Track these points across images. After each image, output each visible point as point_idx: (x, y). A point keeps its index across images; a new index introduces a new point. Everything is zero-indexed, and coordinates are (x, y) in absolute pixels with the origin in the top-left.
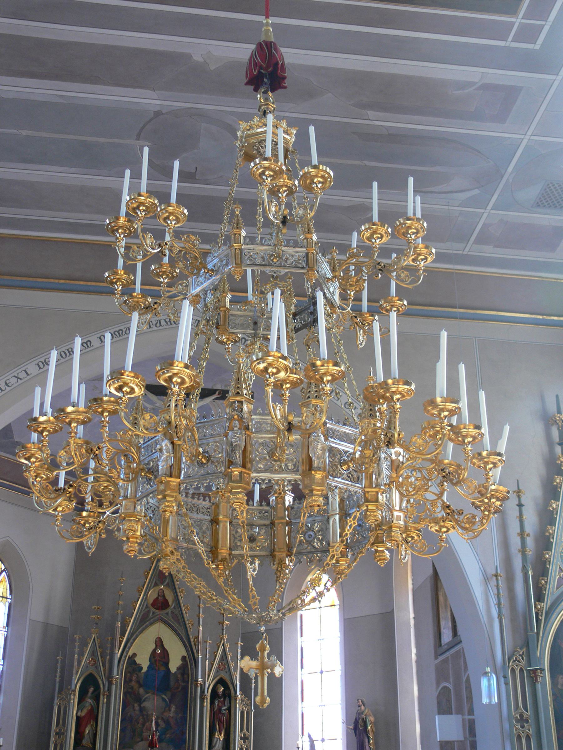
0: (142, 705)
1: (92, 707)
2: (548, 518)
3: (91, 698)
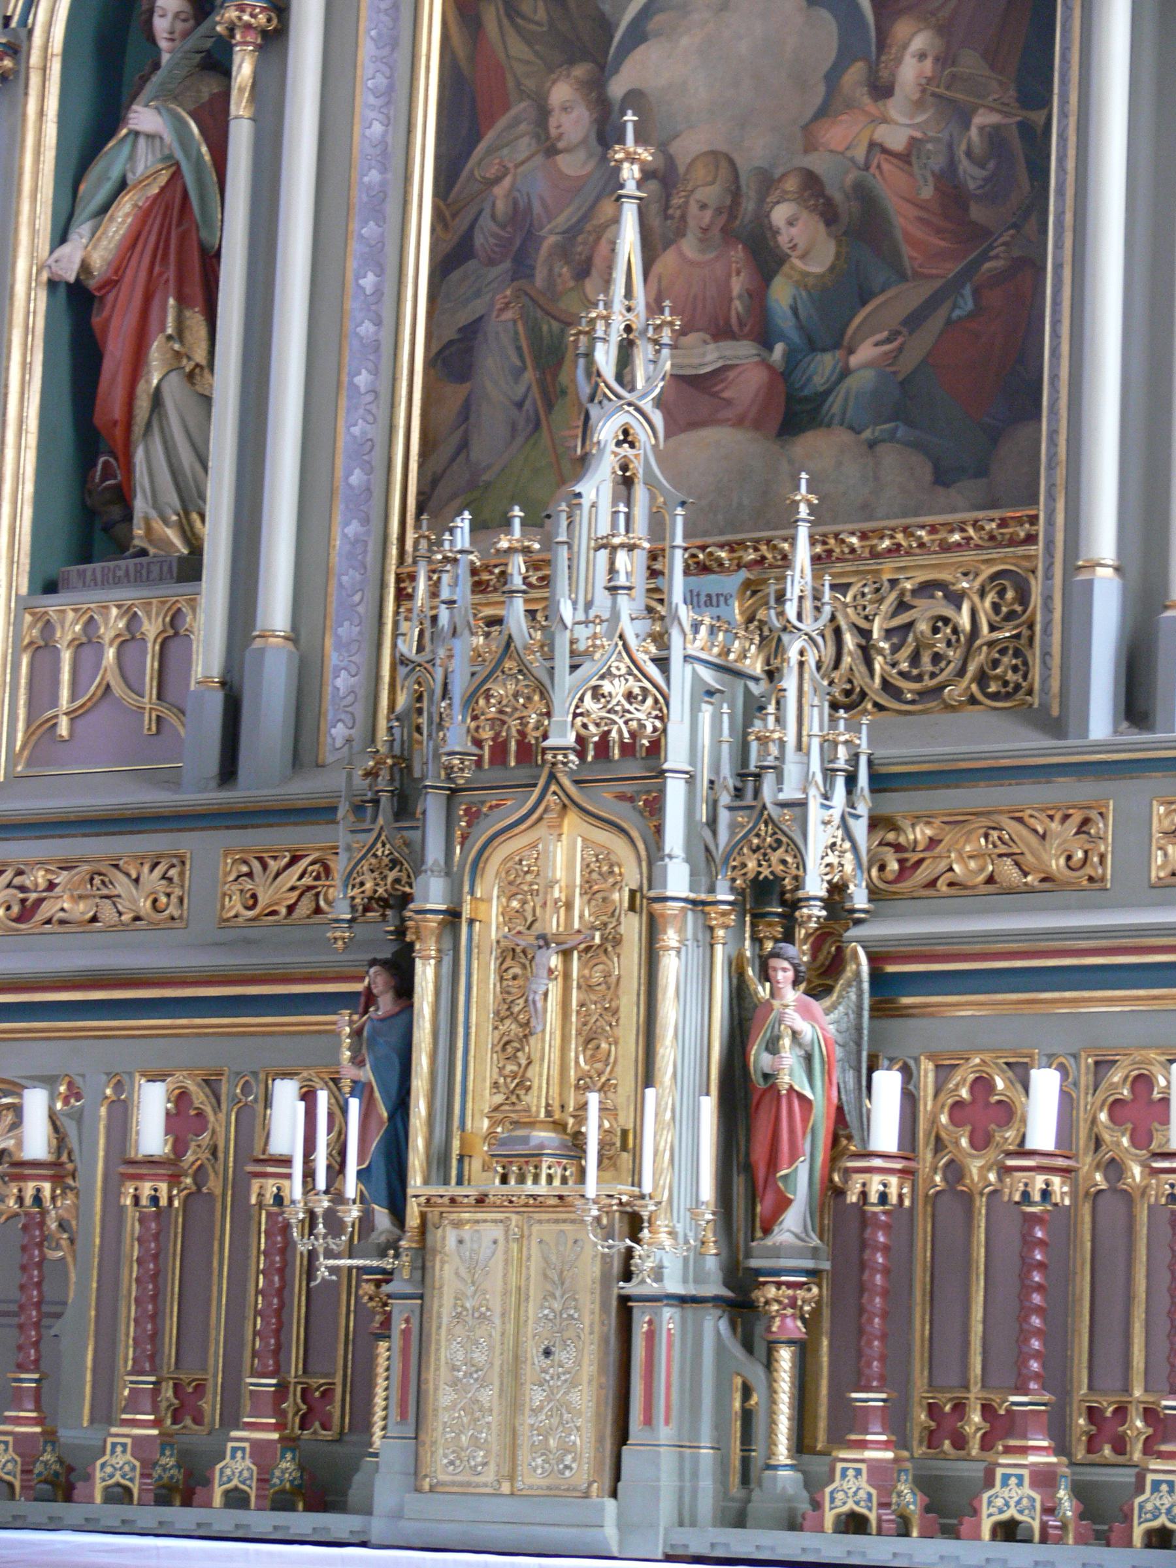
0: (617, 88)
1: (177, 175)
3: (168, 96)
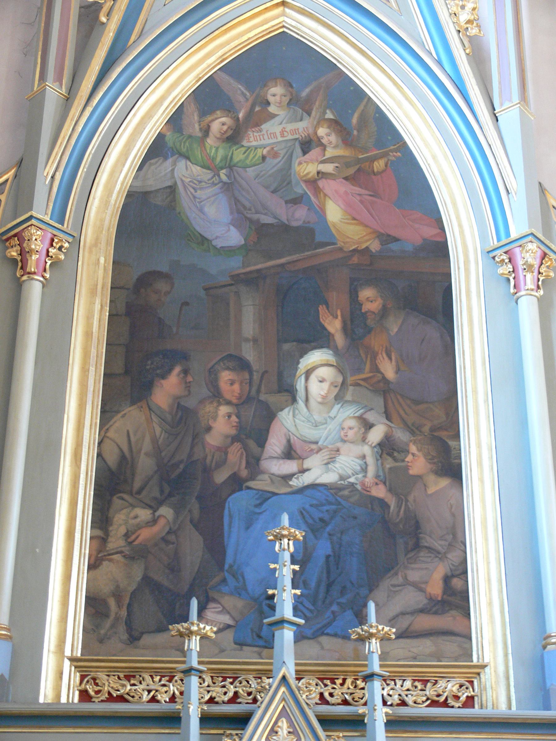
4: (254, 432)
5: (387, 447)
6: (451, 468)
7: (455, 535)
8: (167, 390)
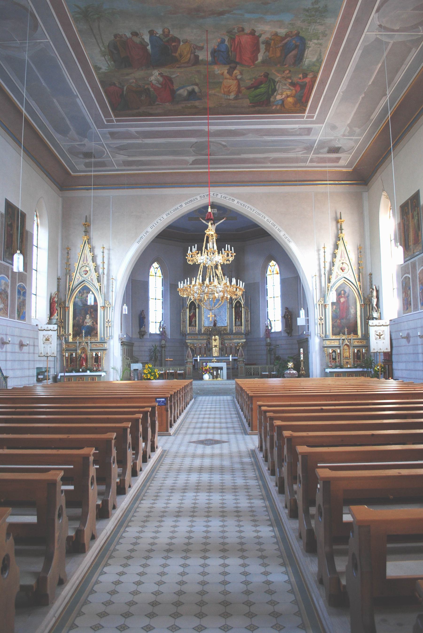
2: (334, 255)
4: (83, 322)
5: (93, 322)
6: (97, 324)
7: (97, 329)
8: (77, 318)
